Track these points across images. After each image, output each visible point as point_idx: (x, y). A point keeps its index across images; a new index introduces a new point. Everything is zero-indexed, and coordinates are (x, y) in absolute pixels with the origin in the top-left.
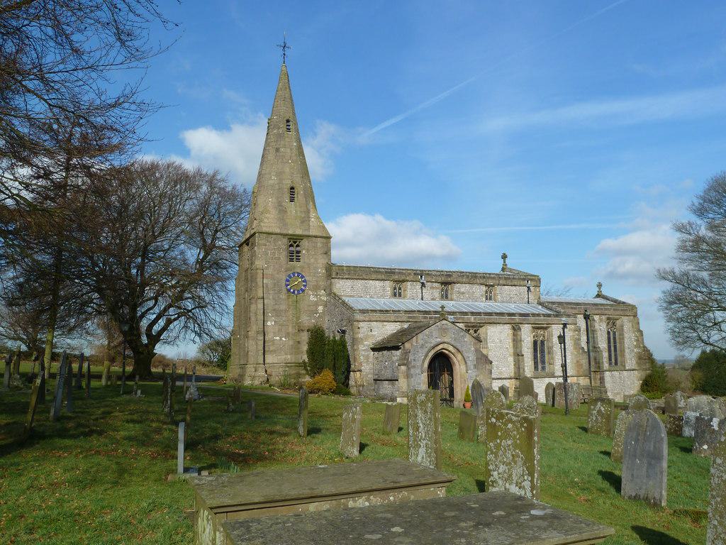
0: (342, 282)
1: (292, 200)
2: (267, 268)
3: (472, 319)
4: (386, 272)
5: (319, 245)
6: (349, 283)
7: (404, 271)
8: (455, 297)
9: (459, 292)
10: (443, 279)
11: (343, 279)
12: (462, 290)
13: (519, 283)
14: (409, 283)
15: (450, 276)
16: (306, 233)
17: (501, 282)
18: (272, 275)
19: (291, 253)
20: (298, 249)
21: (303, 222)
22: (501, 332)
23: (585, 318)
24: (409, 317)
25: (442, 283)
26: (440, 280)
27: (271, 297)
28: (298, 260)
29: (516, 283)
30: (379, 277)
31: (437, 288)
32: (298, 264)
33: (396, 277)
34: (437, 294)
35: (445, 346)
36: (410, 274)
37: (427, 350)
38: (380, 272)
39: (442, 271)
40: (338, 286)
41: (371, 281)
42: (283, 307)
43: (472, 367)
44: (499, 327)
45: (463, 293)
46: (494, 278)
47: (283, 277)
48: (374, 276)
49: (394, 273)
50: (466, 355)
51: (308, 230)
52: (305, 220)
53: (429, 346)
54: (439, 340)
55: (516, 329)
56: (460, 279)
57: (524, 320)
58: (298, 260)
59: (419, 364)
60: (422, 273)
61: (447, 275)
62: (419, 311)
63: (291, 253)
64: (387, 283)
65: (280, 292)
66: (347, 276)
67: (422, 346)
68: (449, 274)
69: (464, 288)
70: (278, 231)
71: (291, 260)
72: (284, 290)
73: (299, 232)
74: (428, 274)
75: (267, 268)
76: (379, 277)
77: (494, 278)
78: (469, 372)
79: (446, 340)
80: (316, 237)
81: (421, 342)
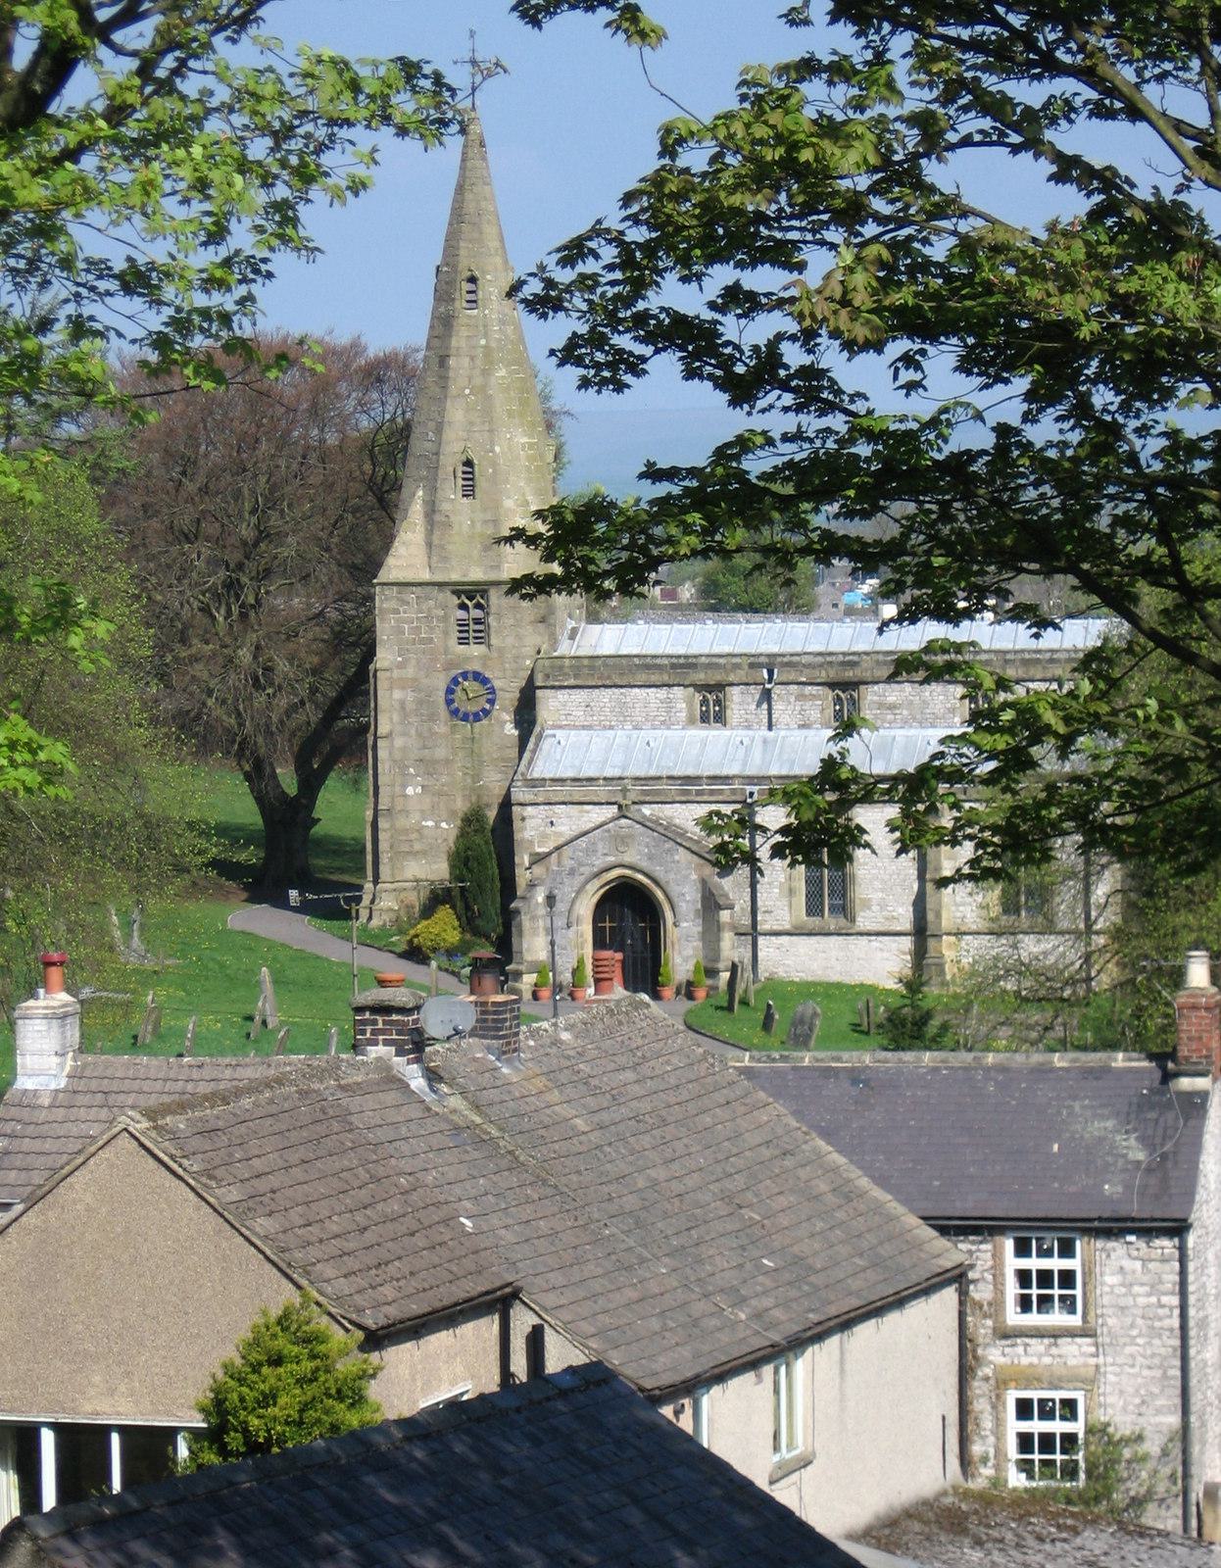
0: (562, 695)
4: (674, 666)
7: (722, 661)
9: (881, 705)
10: (832, 674)
12: (891, 699)
15: (853, 664)
18: (415, 680)
19: (462, 624)
25: (832, 685)
26: (823, 676)
30: (655, 678)
31: (814, 697)
32: (476, 650)
33: (700, 677)
36: (737, 666)
38: (659, 667)
39: (831, 654)
42: (441, 753)
45: (892, 707)
47: (441, 682)
48: (641, 678)
49: (693, 666)
51: (498, 567)
53: (587, 871)
54: (611, 859)
58: (479, 640)
61: (843, 664)
62: (670, 778)
64: (678, 692)
66: (572, 682)
67: (572, 872)
70: (426, 576)
73: (477, 574)
74: (789, 664)
75: (401, 666)
76: (655, 678)
79: (627, 859)
81: (568, 863)
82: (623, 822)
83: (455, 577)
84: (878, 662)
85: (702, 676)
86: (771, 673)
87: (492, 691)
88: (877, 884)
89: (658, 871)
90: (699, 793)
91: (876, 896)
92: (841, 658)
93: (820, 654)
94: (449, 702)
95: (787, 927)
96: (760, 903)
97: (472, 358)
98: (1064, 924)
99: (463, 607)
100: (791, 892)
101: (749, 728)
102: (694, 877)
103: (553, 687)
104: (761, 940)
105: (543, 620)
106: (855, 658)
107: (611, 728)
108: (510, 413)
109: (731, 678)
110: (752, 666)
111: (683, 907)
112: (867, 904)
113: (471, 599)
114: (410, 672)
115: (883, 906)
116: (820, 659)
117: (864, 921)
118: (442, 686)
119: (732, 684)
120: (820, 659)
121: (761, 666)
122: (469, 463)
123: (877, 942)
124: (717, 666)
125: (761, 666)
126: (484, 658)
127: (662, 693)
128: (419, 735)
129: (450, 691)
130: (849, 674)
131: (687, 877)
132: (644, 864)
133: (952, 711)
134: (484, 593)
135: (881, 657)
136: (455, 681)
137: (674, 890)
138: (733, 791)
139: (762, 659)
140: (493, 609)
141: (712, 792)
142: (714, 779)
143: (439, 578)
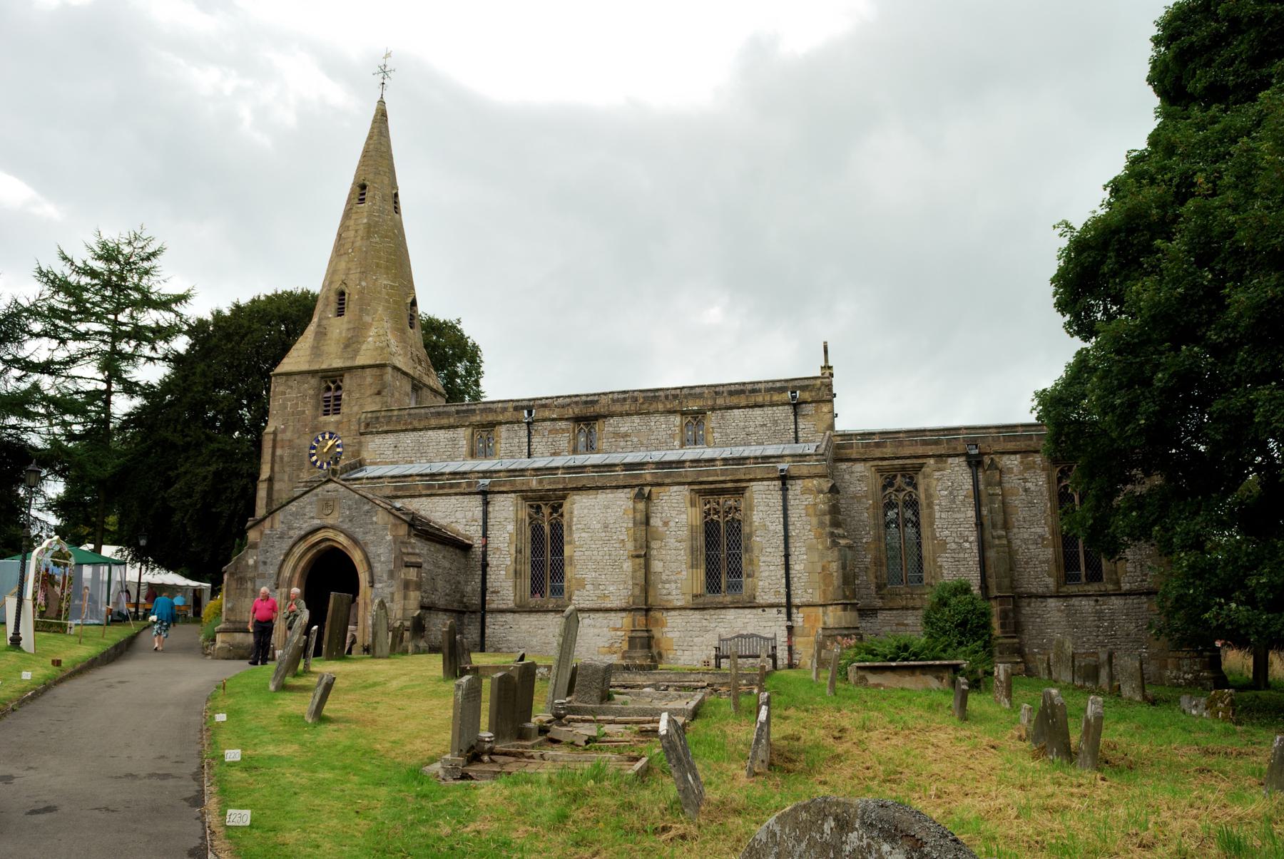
0: (378, 440)
1: (340, 312)
2: (284, 431)
3: (534, 483)
5: (369, 380)
6: (391, 439)
8: (605, 446)
9: (617, 435)
11: (378, 433)
13: (768, 398)
14: (503, 429)
16: (348, 364)
17: (720, 401)
19: (327, 400)
20: (338, 393)
21: (346, 346)
22: (607, 507)
23: (970, 464)
24: (396, 488)
25: (577, 420)
26: (570, 412)
27: (286, 478)
28: (337, 411)
29: (760, 399)
30: (445, 421)
32: (333, 418)
33: (477, 418)
34: (564, 441)
35: (330, 534)
37: (291, 542)
40: (371, 446)
41: (430, 433)
43: (385, 577)
44: (603, 497)
45: (626, 435)
46: (700, 396)
50: (371, 549)
52: (351, 343)
53: (296, 534)
55: (644, 497)
56: (617, 408)
57: (668, 475)
58: (337, 411)
59: (272, 570)
60: (529, 406)
61: (586, 402)
63: (327, 400)
65: (300, 468)
66: (385, 428)
68: (590, 401)
69: (625, 425)
71: (326, 413)
72: (307, 464)
73: (338, 363)
74: (544, 406)
75: (284, 431)
76: (445, 421)
77: (700, 396)
78: (378, 585)
79: (330, 521)
80: (363, 367)
82: (331, 486)
83: (324, 367)
84: (613, 401)
85: (478, 418)
86: (530, 413)
88: (591, 565)
90: (441, 487)
91: (590, 576)
92: (584, 398)
93: (569, 397)
95: (511, 605)
96: (488, 585)
100: (517, 573)
101: (512, 457)
102: (389, 538)
103: (371, 433)
104: (489, 619)
105: (379, 393)
106: (596, 398)
107: (412, 462)
108: (378, 265)
109: (500, 418)
110: (516, 409)
111: (379, 568)
112: (581, 585)
113: (334, 382)
115: (596, 585)
116: (568, 400)
119: (500, 423)
120: (568, 400)
121: (523, 408)
122: (342, 294)
124: (491, 410)
125: (523, 408)
126: (338, 423)
127: (449, 434)
128: (290, 480)
130: (591, 411)
131: (383, 538)
133: (672, 436)
135: (616, 396)
138: (469, 484)
139: (525, 403)
141: (451, 486)
142: (454, 474)
143: (316, 367)
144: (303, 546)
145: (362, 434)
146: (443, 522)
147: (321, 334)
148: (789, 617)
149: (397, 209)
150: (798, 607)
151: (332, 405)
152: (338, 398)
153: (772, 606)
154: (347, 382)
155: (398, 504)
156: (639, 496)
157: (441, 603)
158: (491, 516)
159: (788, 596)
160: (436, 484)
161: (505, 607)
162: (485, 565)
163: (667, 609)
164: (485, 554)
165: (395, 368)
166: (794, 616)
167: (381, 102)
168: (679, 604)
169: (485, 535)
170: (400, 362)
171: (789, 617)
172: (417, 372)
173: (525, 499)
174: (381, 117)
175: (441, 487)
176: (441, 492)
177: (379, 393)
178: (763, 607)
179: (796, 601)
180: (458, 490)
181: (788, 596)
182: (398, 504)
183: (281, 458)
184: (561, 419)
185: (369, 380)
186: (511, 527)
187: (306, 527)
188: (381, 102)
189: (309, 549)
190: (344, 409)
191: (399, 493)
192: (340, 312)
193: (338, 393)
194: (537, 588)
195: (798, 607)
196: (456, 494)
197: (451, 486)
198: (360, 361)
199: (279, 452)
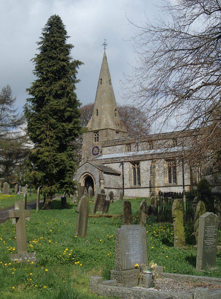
1: (97, 115)
3: (132, 160)
5: (104, 133)
19: (95, 138)
25: (148, 142)
28: (98, 141)
30: (120, 143)
32: (97, 143)
37: (80, 175)
52: (99, 124)
53: (81, 174)
58: (98, 141)
73: (97, 129)
75: (86, 146)
79: (87, 171)
80: (103, 130)
83: (94, 130)
87: (99, 149)
89: (93, 174)
90: (114, 161)
94: (93, 152)
95: (129, 187)
96: (124, 183)
97: (100, 92)
98: (179, 184)
99: (96, 135)
100: (130, 180)
102: (98, 174)
103: (104, 147)
104: (125, 190)
105: (106, 136)
106: (152, 136)
114: (87, 147)
117: (142, 186)
118: (92, 150)
119: (131, 143)
122: (97, 110)
123: (145, 190)
129: (93, 150)
132: (90, 172)
134: (98, 132)
136: (94, 148)
137: (95, 177)
140: (99, 135)
141: (116, 161)
144: (83, 176)
145: (102, 147)
146: (115, 169)
147: (93, 121)
148: (184, 188)
149: (110, 84)
150: (186, 186)
151: (97, 139)
152: (98, 137)
153: (180, 186)
154: (100, 133)
155: (105, 165)
156: (152, 162)
157: (113, 187)
158: (124, 167)
159: (184, 183)
160: (113, 160)
161: (128, 187)
162: (123, 178)
163: (160, 187)
164: (123, 176)
165: (110, 129)
166: (185, 188)
167: (105, 54)
168: (162, 186)
169: (123, 172)
170: (113, 126)
171: (184, 188)
172: (118, 128)
173: (131, 163)
174: (105, 58)
175: (114, 161)
176: (114, 162)
177: (106, 136)
178: (179, 186)
179: (185, 184)
180: (117, 162)
181: (184, 183)
182: (105, 165)
183: (86, 153)
184: (144, 142)
185: (104, 133)
186: (128, 169)
187: (83, 172)
188: (105, 54)
189: (84, 177)
190: (99, 140)
191: (106, 163)
192: (97, 115)
193: (98, 136)
194: (135, 184)
195: (186, 186)
196: (117, 162)
197: (116, 161)
198: (102, 128)
199: (85, 152)
